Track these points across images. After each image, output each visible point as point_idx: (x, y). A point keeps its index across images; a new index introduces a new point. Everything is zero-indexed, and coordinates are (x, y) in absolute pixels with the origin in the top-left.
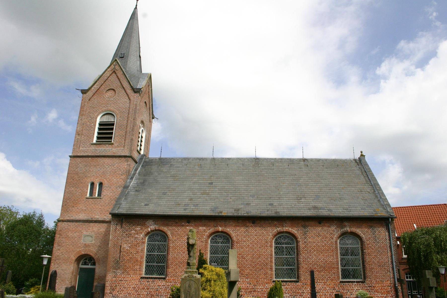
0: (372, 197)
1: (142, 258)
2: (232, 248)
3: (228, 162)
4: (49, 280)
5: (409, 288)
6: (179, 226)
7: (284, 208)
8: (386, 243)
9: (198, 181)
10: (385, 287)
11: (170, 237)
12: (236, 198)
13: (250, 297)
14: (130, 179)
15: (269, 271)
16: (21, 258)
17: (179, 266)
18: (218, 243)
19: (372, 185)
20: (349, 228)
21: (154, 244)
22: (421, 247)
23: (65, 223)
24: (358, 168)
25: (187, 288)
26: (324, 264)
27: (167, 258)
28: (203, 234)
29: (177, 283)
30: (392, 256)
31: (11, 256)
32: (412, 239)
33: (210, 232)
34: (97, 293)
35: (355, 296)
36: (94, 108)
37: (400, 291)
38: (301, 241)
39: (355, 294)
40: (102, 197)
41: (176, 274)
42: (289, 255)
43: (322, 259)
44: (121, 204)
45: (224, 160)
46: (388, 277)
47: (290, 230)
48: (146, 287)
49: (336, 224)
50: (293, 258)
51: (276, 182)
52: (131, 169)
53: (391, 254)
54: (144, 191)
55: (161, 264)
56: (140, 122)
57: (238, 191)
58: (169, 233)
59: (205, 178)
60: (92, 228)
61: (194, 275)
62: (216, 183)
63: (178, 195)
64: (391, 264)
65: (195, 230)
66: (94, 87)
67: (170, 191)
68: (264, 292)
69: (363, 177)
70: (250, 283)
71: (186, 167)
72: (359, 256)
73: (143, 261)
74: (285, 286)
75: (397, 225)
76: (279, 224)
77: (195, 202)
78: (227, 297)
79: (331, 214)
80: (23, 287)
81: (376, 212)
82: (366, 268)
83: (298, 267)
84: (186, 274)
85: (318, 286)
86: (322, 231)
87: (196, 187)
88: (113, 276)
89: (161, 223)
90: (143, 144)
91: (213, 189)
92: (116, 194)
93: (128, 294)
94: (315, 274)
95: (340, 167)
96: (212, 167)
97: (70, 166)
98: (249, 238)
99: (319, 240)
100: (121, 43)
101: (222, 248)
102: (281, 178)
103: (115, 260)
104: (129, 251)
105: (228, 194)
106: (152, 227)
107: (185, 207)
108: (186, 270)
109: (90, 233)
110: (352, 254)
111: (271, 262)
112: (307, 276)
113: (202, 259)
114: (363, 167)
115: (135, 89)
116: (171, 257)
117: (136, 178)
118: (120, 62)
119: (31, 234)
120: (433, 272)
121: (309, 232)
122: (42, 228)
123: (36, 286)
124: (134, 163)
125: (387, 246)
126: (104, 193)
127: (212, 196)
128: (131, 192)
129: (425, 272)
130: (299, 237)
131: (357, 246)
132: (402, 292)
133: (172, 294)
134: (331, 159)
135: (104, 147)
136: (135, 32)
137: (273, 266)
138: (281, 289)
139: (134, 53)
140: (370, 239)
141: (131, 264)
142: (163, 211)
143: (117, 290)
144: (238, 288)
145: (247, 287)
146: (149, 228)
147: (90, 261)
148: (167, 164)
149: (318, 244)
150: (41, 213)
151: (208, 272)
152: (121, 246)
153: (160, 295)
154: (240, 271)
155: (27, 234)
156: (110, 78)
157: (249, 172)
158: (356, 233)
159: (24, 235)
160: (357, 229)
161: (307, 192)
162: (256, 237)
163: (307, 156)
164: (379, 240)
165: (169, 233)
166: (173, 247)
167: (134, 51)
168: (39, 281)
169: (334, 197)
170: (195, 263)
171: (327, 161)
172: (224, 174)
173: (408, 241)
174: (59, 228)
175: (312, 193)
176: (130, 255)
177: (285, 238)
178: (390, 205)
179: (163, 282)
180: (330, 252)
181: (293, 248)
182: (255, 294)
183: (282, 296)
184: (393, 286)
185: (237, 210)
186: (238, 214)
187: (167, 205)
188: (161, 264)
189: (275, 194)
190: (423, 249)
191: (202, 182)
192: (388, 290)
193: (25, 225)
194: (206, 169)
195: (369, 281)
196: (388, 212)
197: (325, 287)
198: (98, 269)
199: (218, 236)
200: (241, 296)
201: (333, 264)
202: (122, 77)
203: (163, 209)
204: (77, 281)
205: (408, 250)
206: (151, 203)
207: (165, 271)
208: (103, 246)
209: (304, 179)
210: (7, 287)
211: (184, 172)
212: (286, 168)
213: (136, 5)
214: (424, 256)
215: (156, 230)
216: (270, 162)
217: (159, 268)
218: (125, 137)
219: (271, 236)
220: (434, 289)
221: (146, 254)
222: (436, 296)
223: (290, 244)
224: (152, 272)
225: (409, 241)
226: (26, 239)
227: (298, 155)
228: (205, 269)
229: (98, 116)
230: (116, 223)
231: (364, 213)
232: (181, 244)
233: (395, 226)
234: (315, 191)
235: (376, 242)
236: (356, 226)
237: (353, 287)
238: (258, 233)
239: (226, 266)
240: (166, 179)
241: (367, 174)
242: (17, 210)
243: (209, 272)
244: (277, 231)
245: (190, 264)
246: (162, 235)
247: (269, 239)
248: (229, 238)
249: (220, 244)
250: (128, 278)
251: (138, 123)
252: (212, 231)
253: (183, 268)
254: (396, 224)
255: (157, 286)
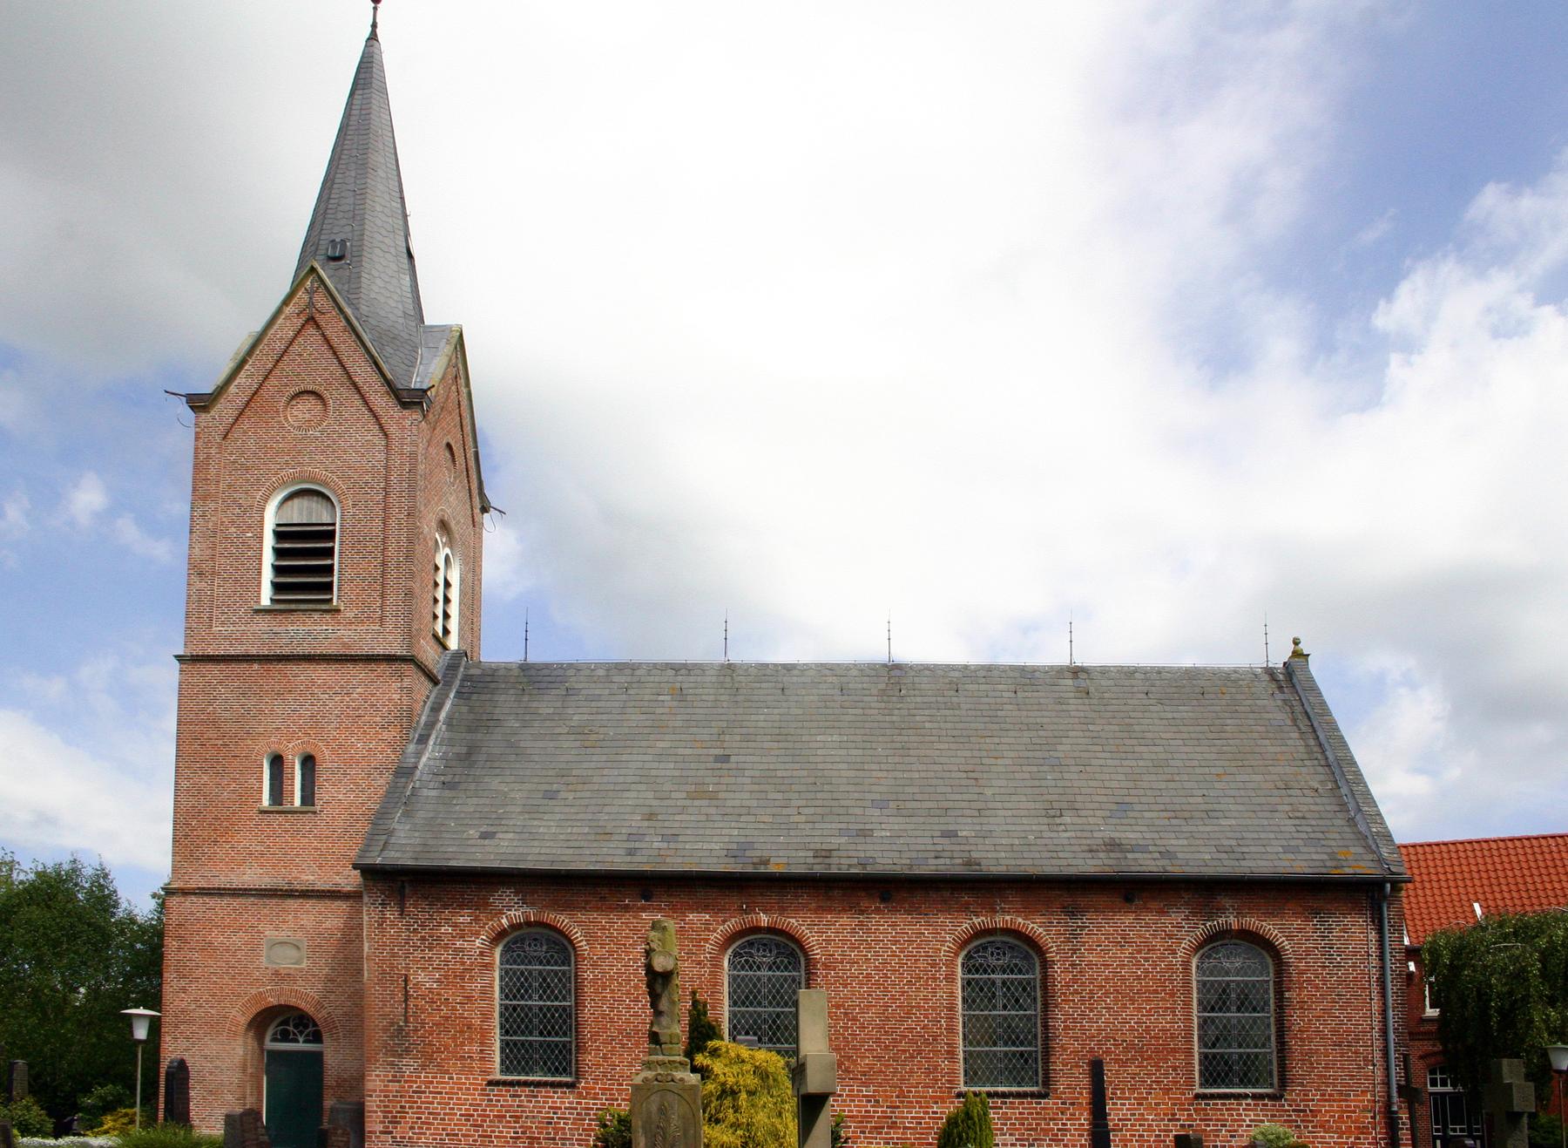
0: (1328, 808)
1: (486, 1017)
2: (809, 984)
3: (785, 678)
4: (162, 1091)
5: (1440, 1117)
6: (611, 909)
7: (998, 848)
8: (1366, 967)
9: (672, 751)
10: (1354, 1112)
11: (582, 946)
12: (819, 810)
13: (876, 1143)
14: (416, 743)
15: (944, 1062)
16: (52, 1016)
17: (621, 1044)
18: (759, 968)
19: (1329, 766)
20: (1235, 917)
21: (526, 970)
22: (1493, 981)
23: (194, 898)
24: (1279, 703)
25: (655, 1117)
26: (1141, 1037)
27: (576, 1018)
28: (703, 939)
29: (617, 1100)
30: (1384, 1012)
31: (15, 1011)
32: (1461, 954)
33: (726, 930)
34: (340, 1131)
35: (1245, 1142)
36: (247, 469)
37: (1405, 1127)
38: (1058, 961)
39: (1245, 1134)
40: (318, 808)
41: (612, 1069)
42: (1013, 1008)
43: (1135, 1023)
44: (392, 832)
45: (768, 672)
46: (1365, 1080)
47: (1020, 923)
48: (508, 1115)
49: (1187, 904)
50: (1029, 1018)
51: (968, 754)
52: (418, 707)
53: (1384, 1004)
54: (473, 786)
55: (557, 1039)
56: (434, 524)
57: (826, 788)
58: (577, 932)
59: (698, 737)
60: (296, 918)
61: (678, 1075)
62: (742, 759)
63: (600, 802)
64: (1379, 1040)
65: (671, 925)
66: (236, 383)
67: (570, 787)
68: (926, 1128)
69: (1296, 735)
70: (878, 1101)
71: (624, 697)
72: (1268, 1013)
73: (493, 1029)
74: (1001, 1111)
75: (1413, 905)
76: (980, 905)
77: (666, 824)
78: (797, 1144)
79: (1169, 869)
80: (77, 1113)
81: (1339, 860)
82: (1288, 1053)
83: (1048, 1048)
84: (649, 1072)
85: (1116, 1111)
86: (1135, 927)
87: (668, 773)
88: (388, 1076)
89: (545, 900)
90: (454, 610)
91: (733, 780)
92: (369, 799)
93: (447, 1135)
94: (1108, 1070)
95: (1213, 696)
96: (722, 698)
97: (185, 694)
98: (870, 952)
99: (1125, 957)
100: (325, 197)
101: (774, 986)
102: (988, 740)
103: (391, 1026)
104: (438, 994)
105: (787, 795)
106: (515, 915)
107: (632, 845)
108: (646, 1059)
109: (289, 933)
110: (1243, 1003)
111: (951, 1030)
112: (1078, 1077)
113: (702, 1023)
114: (1300, 697)
115: (405, 393)
116: (591, 1014)
117: (437, 738)
118: (329, 278)
119: (75, 937)
120: (1528, 1064)
121: (1089, 931)
122: (112, 917)
123: (119, 1110)
124: (428, 685)
125: (1369, 978)
126: (323, 794)
127: (729, 803)
128: (425, 790)
129: (1500, 1066)
130: (1052, 947)
131: (1261, 979)
132: (1413, 1129)
133: (602, 1134)
134: (1180, 668)
135: (304, 623)
136: (381, 146)
137: (956, 1044)
138: (986, 1121)
139: (386, 240)
140: (1310, 955)
141: (448, 1038)
142: (551, 858)
143: (407, 1123)
144: (833, 1116)
145: (866, 1111)
146: (504, 916)
147: (301, 1028)
148: (550, 686)
149: (1119, 970)
150: (101, 865)
151: (726, 1065)
152: (406, 978)
153: (560, 1139)
154: (838, 1060)
155: (59, 938)
156: (295, 348)
157: (864, 718)
158: (1258, 934)
159: (48, 940)
160: (1266, 921)
161: (1083, 791)
162: (894, 947)
163: (1092, 655)
164: (1343, 957)
165: (577, 932)
166: (594, 981)
167: (384, 233)
168: (128, 1093)
169: (1184, 807)
170: (677, 1035)
171: (1164, 675)
172: (770, 724)
173: (1448, 962)
174: (174, 917)
175: (1103, 791)
176: (442, 1008)
177: (1000, 949)
178: (1390, 836)
179: (568, 1098)
180: (1163, 999)
181: (1029, 983)
182: (895, 1136)
183: (989, 1142)
184: (1383, 1110)
185: (824, 854)
186: (827, 866)
187: (562, 837)
188: (557, 1039)
189: (965, 797)
190: (1499, 988)
191: (689, 751)
192: (1365, 1123)
193: (49, 907)
194: (700, 704)
195: (1297, 1095)
196: (1381, 860)
197: (1143, 1114)
198: (334, 1057)
199: (756, 945)
200: (846, 1142)
201: (1172, 1038)
202: (344, 342)
203: (548, 851)
204: (262, 1095)
205: (1443, 990)
206: (505, 829)
207: (574, 1061)
208: (341, 978)
209: (1075, 741)
210: (20, 1113)
211: (618, 717)
212: (1005, 700)
213: (374, 26)
214: (1500, 1011)
215: (528, 924)
216: (947, 681)
217: (549, 1052)
218: (383, 585)
219: (951, 945)
220: (1525, 1120)
221: (501, 1005)
222: (1530, 1143)
223: (1020, 972)
224: (527, 1063)
225: (1451, 963)
226: (59, 955)
227: (1052, 653)
228: (715, 1053)
229: (266, 501)
230: (380, 899)
231: (1294, 864)
232: (623, 971)
233: (1406, 911)
234: (1114, 784)
235: (1333, 963)
236: (1260, 910)
237: (1241, 1111)
238: (903, 933)
239: (790, 1044)
240: (551, 744)
241: (1312, 725)
242: (10, 854)
243: (731, 1063)
244: (971, 927)
245: (660, 1040)
246: (554, 942)
247: (942, 953)
248: (798, 951)
249: (765, 973)
250: (442, 1083)
251: (426, 529)
252: (733, 925)
253: (634, 1051)
254: (1410, 903)
255: (547, 1110)
